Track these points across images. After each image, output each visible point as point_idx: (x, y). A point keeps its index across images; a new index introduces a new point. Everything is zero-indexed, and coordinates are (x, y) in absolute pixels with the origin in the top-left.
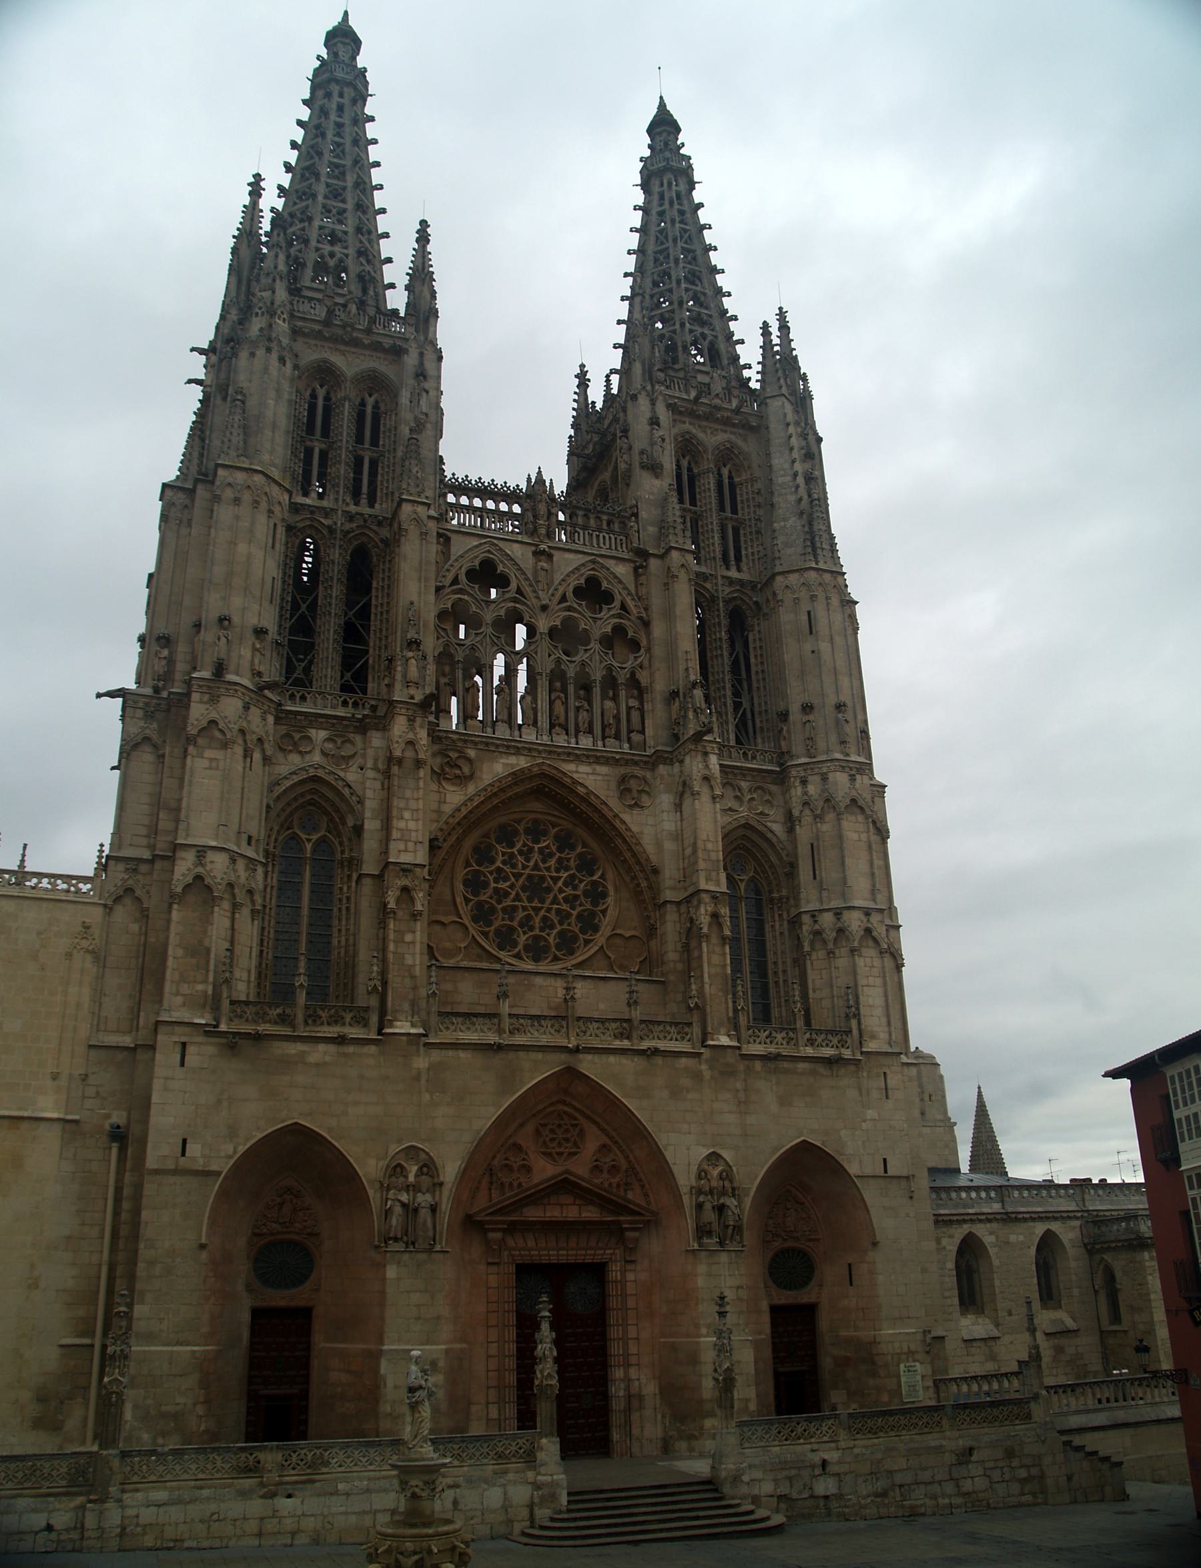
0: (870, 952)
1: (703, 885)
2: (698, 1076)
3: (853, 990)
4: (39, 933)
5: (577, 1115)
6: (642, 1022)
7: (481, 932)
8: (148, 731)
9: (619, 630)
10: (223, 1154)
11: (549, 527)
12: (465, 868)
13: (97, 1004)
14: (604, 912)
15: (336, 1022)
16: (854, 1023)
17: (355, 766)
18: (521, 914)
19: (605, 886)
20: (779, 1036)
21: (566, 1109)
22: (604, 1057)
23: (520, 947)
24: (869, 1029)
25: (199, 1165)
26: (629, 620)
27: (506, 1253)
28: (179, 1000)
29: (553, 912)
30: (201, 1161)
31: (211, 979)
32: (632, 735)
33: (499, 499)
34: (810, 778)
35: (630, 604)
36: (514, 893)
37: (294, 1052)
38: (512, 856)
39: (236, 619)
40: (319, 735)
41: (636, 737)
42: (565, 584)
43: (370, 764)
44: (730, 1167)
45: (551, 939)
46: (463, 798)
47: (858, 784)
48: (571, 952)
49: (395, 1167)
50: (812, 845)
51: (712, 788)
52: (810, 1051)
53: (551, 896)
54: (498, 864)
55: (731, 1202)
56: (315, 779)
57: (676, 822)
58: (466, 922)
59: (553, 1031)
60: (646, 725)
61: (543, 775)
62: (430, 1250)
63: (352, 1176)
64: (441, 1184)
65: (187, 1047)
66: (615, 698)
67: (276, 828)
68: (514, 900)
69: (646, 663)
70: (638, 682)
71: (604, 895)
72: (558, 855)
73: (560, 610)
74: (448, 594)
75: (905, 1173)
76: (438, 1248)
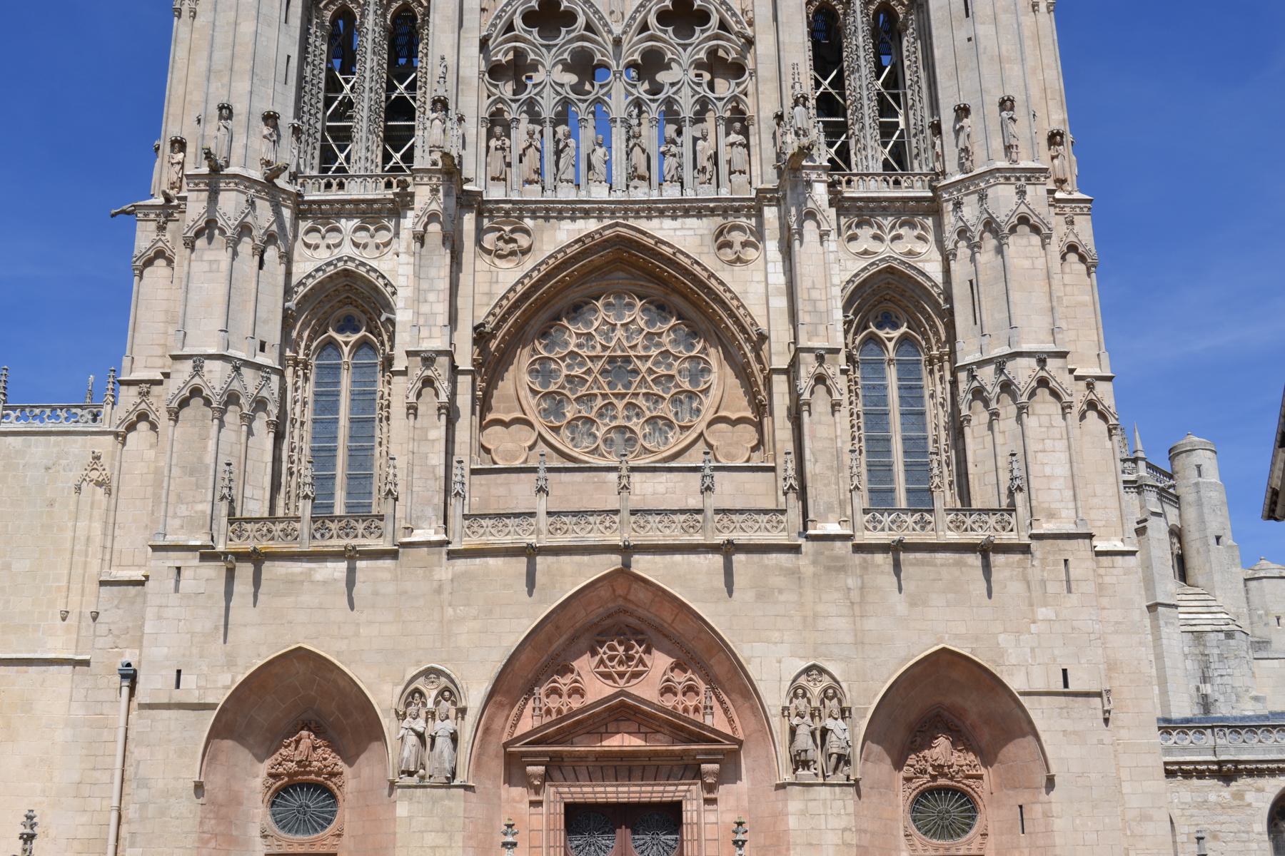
0: (1045, 407)
1: (803, 343)
2: (794, 573)
3: (1021, 457)
4: (47, 468)
5: (644, 627)
6: (717, 511)
7: (549, 427)
8: (160, 244)
10: (220, 685)
12: (532, 356)
13: (110, 538)
14: (706, 391)
15: (347, 535)
16: (1019, 498)
18: (599, 402)
19: (706, 362)
20: (910, 520)
21: (631, 621)
22: (668, 558)
23: (599, 441)
24: (1046, 505)
25: (193, 699)
26: (729, 40)
27: (552, 789)
28: (177, 522)
30: (197, 693)
31: (210, 498)
32: (732, 176)
34: (965, 200)
35: (731, 21)
36: (590, 380)
37: (299, 570)
38: (589, 336)
39: (239, 108)
40: (347, 225)
43: (402, 249)
44: (838, 682)
46: (518, 274)
47: (1028, 198)
49: (412, 694)
50: (971, 282)
51: (819, 226)
52: (953, 537)
53: (639, 378)
54: (572, 348)
55: (835, 725)
56: (346, 273)
58: (531, 418)
59: (601, 528)
61: (619, 239)
62: (448, 783)
63: (366, 706)
64: (463, 711)
65: (182, 571)
67: (306, 334)
68: (591, 388)
69: (751, 90)
73: (641, 41)
74: (501, 44)
75: (1095, 688)
76: (456, 782)
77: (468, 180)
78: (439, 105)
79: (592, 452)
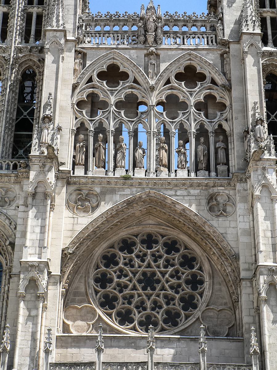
9: (210, 98)
11: (156, 35)
12: (96, 269)
14: (201, 295)
17: (14, 205)
23: (136, 322)
29: (161, 296)
33: (122, 23)
41: (221, 168)
42: (168, 72)
45: (159, 317)
48: (175, 324)
57: (249, 222)
60: (230, 159)
66: (207, 143)
70: (224, 131)
71: (202, 282)
72: (166, 255)
77: (63, 164)
78: (47, 120)
79: (131, 329)
